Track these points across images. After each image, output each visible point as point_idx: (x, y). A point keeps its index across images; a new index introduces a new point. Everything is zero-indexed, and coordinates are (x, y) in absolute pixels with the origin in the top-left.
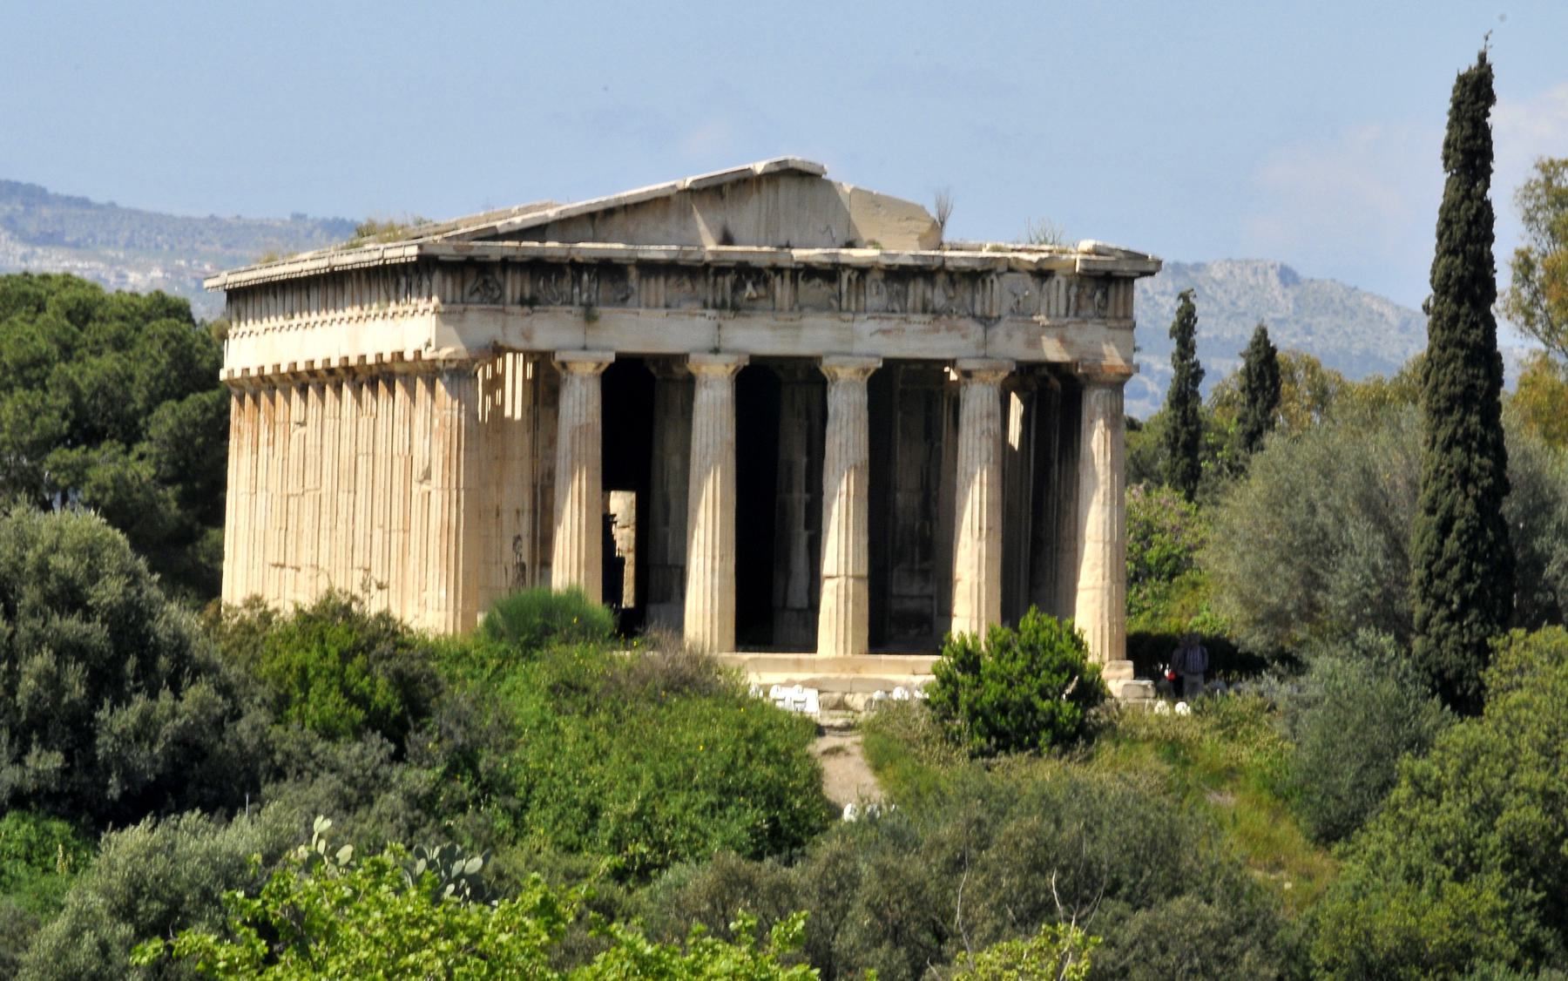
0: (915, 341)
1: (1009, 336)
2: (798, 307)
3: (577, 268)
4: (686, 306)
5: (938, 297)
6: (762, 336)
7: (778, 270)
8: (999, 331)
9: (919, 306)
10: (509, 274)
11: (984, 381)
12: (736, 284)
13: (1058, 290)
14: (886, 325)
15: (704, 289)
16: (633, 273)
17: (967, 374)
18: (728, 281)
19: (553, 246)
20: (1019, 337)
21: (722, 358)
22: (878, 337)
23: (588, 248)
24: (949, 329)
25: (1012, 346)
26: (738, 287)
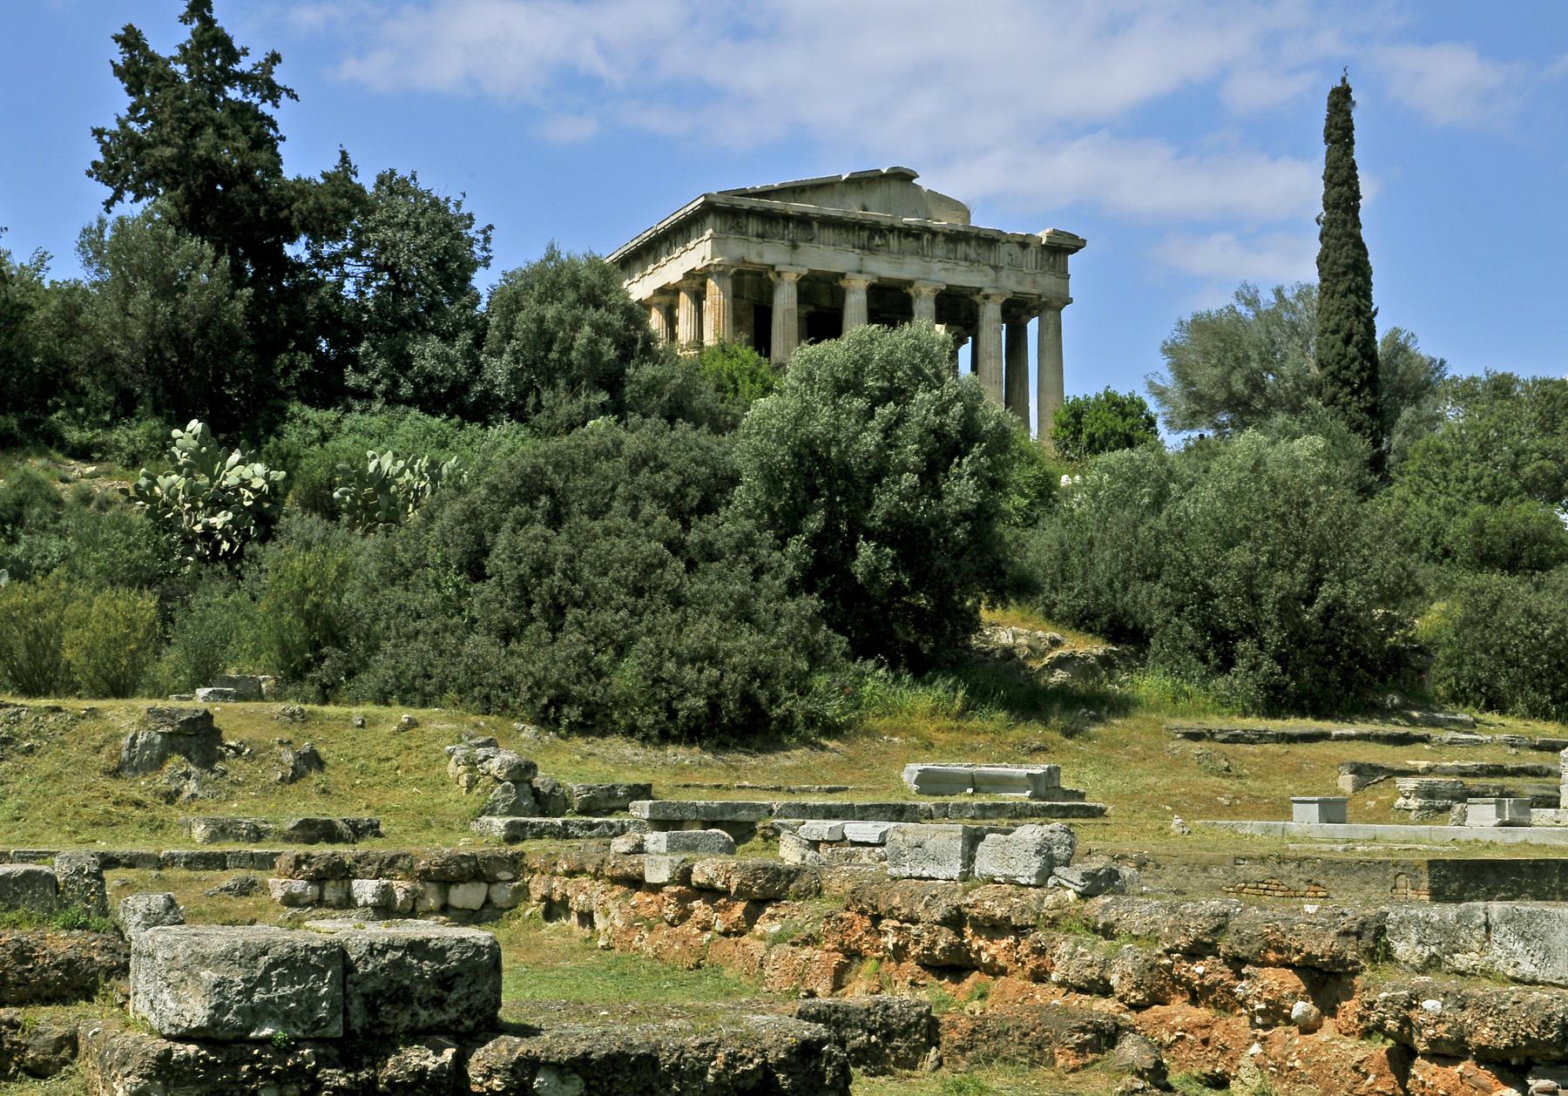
0: (962, 277)
2: (901, 252)
3: (787, 218)
4: (844, 246)
5: (972, 254)
6: (884, 267)
7: (892, 229)
8: (1003, 274)
12: (869, 234)
13: (1031, 256)
15: (853, 238)
16: (816, 226)
17: (987, 297)
18: (865, 234)
19: (776, 204)
20: (1013, 279)
21: (863, 276)
23: (796, 206)
25: (1011, 284)
26: (871, 238)
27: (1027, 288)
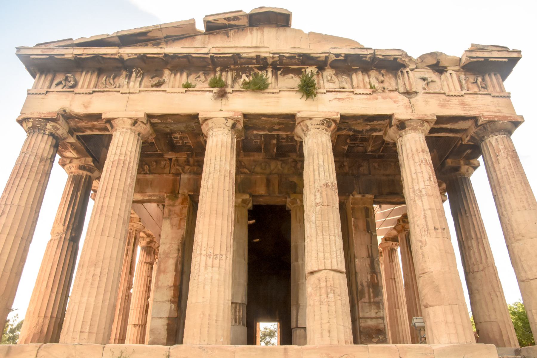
1: (427, 102)
8: (419, 100)
9: (361, 85)
10: (84, 73)
11: (415, 129)
14: (339, 95)
22: (335, 102)
24: (384, 98)
27: (454, 109)
